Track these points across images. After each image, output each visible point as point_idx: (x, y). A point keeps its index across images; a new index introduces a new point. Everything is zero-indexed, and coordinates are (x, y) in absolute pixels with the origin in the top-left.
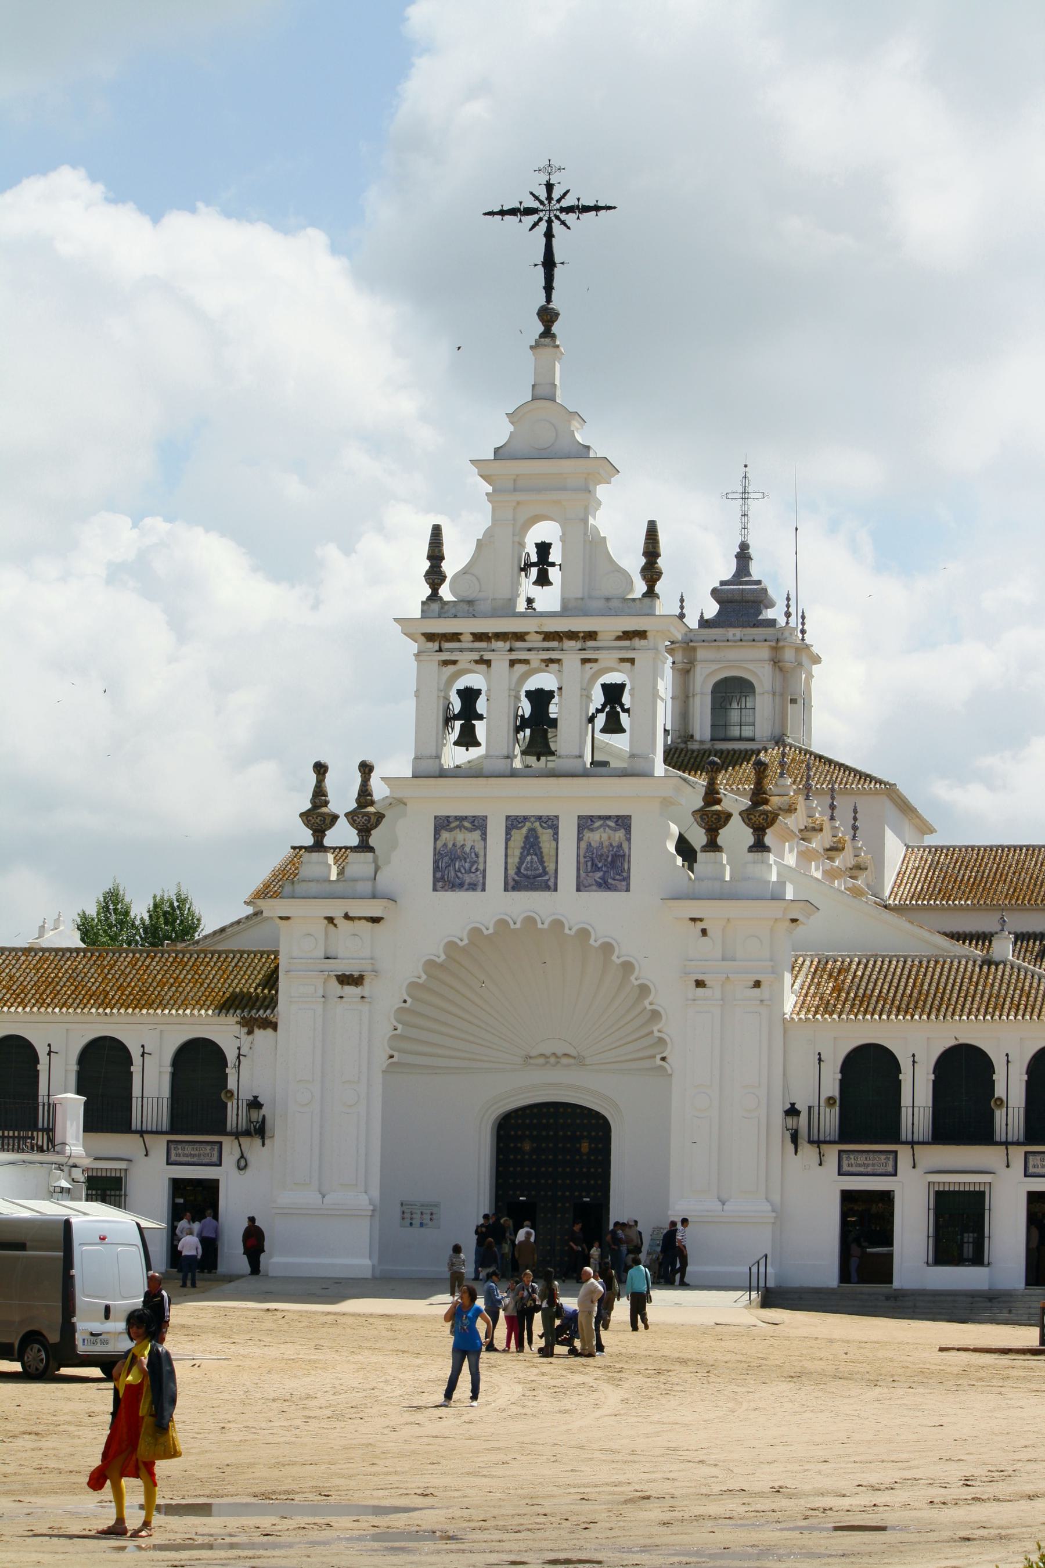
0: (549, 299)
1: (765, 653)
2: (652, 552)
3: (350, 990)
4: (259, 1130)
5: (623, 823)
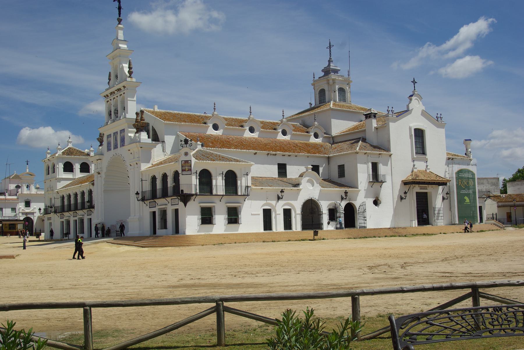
0: (120, 16)
1: (326, 82)
2: (130, 68)
3: (99, 175)
4: (93, 207)
5: (124, 130)
